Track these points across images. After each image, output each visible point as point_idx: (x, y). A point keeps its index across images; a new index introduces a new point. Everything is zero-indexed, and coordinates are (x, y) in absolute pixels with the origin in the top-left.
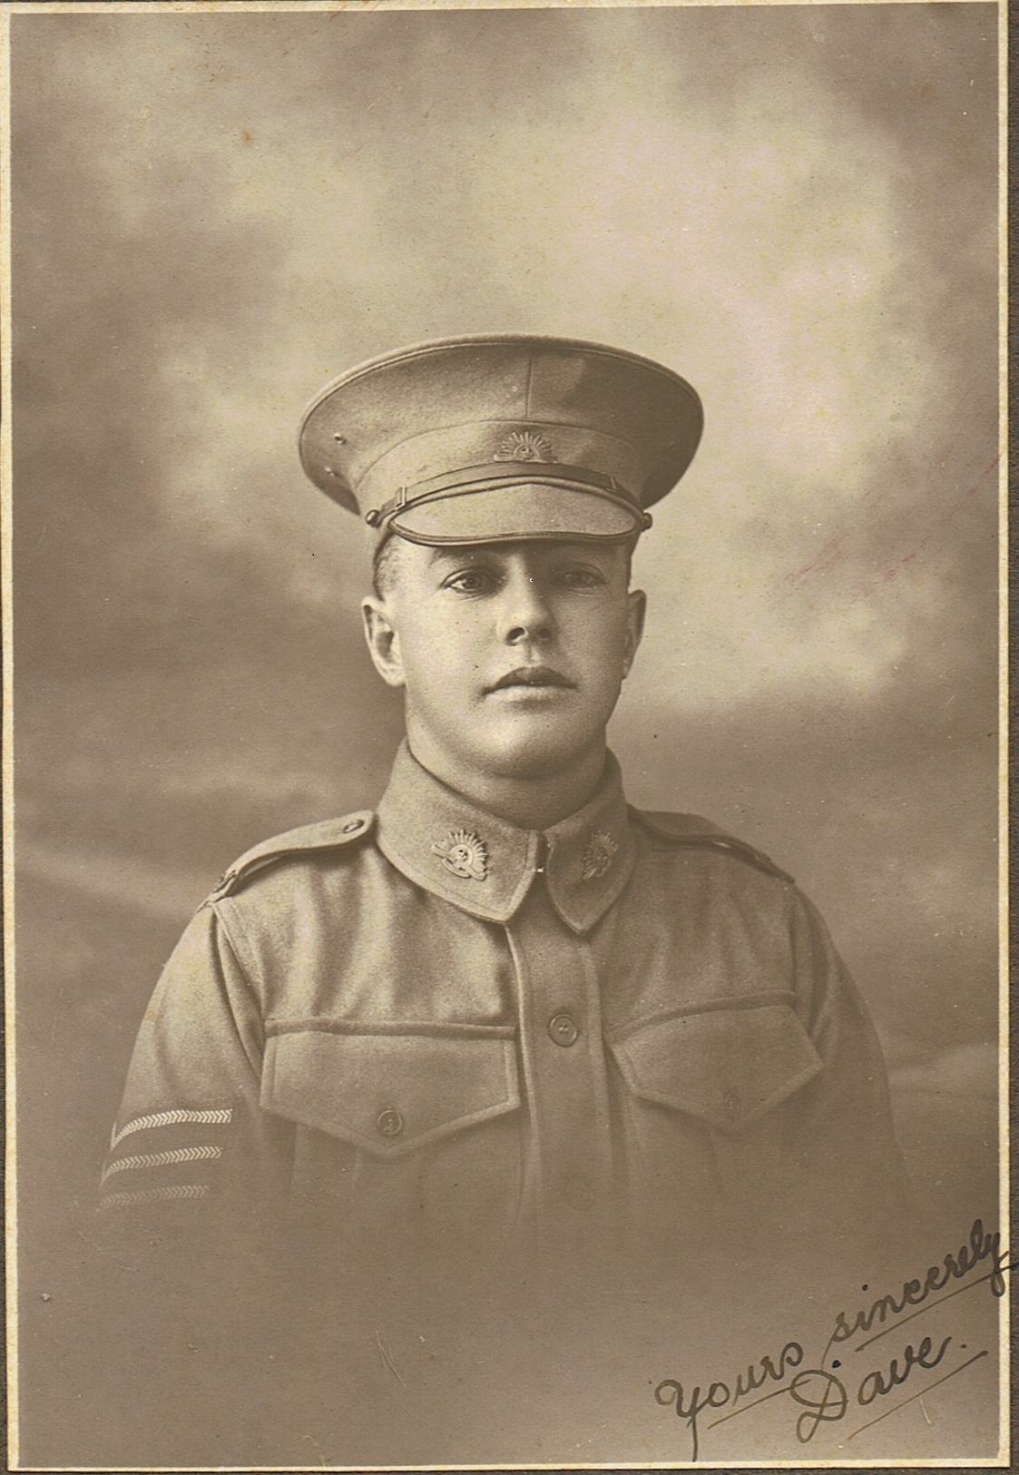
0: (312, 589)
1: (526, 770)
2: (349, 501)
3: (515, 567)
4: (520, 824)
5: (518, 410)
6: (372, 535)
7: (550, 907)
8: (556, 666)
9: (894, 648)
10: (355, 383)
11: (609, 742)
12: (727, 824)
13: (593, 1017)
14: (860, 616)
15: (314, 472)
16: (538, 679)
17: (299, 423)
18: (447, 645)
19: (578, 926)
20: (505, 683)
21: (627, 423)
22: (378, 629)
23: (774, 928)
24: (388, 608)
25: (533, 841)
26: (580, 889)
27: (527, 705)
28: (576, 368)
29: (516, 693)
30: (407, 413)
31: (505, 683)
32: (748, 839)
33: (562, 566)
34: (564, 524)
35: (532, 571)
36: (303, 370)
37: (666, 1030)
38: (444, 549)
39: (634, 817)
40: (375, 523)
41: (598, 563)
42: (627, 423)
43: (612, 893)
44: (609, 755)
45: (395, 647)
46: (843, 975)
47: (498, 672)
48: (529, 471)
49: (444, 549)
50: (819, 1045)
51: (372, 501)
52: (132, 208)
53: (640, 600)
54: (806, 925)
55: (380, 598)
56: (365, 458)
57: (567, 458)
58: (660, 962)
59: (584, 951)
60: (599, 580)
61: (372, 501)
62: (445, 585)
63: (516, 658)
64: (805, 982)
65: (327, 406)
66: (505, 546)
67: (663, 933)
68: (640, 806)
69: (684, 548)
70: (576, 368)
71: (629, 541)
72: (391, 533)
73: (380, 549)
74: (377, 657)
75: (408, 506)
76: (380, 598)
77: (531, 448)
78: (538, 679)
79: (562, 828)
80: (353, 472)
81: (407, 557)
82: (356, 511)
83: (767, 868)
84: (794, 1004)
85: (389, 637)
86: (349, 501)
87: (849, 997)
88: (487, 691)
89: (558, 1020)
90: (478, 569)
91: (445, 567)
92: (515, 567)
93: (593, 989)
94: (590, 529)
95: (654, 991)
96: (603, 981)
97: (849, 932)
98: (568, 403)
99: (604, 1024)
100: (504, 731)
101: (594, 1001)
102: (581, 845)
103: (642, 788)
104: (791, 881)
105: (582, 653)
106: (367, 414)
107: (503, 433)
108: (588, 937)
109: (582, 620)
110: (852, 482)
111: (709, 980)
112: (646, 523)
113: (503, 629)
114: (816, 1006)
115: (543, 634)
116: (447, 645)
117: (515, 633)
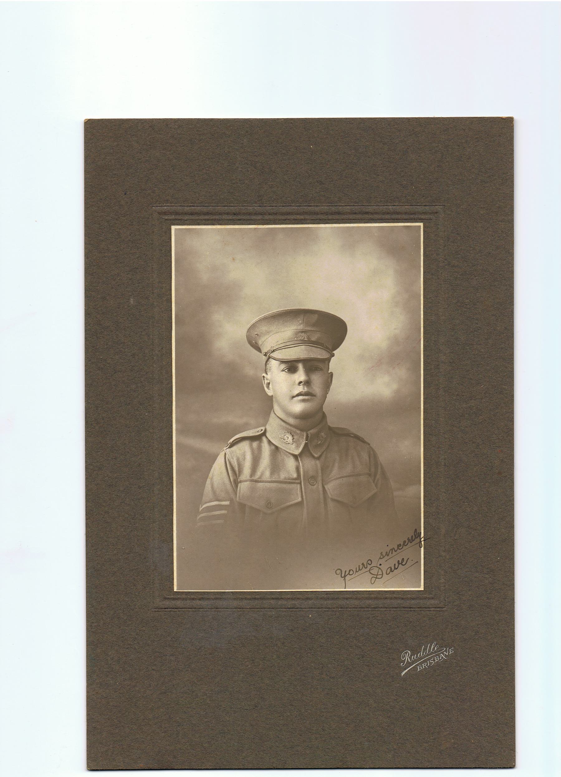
0: (250, 371)
1: (303, 417)
2: (259, 350)
3: (300, 366)
4: (302, 430)
5: (301, 327)
6: (265, 358)
7: (309, 451)
8: (310, 391)
9: (395, 386)
10: (260, 320)
11: (324, 410)
12: (353, 430)
13: (320, 478)
14: (386, 378)
15: (250, 343)
16: (306, 394)
17: (246, 330)
18: (283, 385)
19: (316, 456)
20: (298, 395)
21: (328, 330)
22: (266, 381)
23: (365, 456)
24: (269, 376)
25: (305, 434)
26: (317, 446)
27: (303, 401)
28: (316, 317)
29: (301, 398)
30: (273, 328)
31: (298, 395)
32: (359, 434)
33: (313, 366)
34: (313, 356)
35: (305, 367)
36: (247, 317)
37: (338, 482)
38: (283, 362)
39: (330, 428)
40: (265, 355)
41: (321, 365)
42: (328, 330)
43: (324, 448)
44: (324, 413)
45: (270, 386)
46: (382, 468)
47: (296, 392)
48: (303, 342)
49: (283, 362)
50: (376, 486)
51: (264, 350)
52: (205, 277)
53: (332, 374)
54: (373, 455)
55: (267, 374)
56: (263, 339)
57: (313, 339)
58: (337, 465)
59: (318, 462)
60: (321, 370)
61: (264, 350)
62: (283, 371)
63: (300, 389)
64: (373, 470)
65: (254, 326)
66: (298, 361)
67: (337, 457)
68: (331, 426)
69: (343, 361)
70: (316, 317)
71: (329, 360)
72: (269, 358)
73: (267, 362)
74: (266, 389)
75: (274, 351)
76: (267, 374)
77: (304, 336)
78: (306, 394)
79: (312, 431)
80: (260, 342)
81: (274, 364)
82: (261, 352)
83: (363, 441)
84: (370, 475)
85: (269, 384)
86: (259, 350)
87: (383, 473)
88: (293, 397)
89: (311, 479)
90: (291, 367)
91: (283, 366)
92: (300, 366)
93: (320, 471)
94: (319, 357)
95: (335, 472)
96: (322, 470)
97: (383, 457)
98: (314, 325)
99: (322, 480)
100: (298, 407)
101: (320, 474)
102: (317, 435)
103: (332, 421)
104: (369, 444)
105: (317, 388)
106: (263, 328)
107: (297, 333)
108: (318, 458)
109: (317, 379)
110: (384, 345)
111: (349, 469)
112: (333, 355)
113: (297, 382)
114: (375, 476)
115: (307, 383)
116: (283, 385)
117: (300, 383)
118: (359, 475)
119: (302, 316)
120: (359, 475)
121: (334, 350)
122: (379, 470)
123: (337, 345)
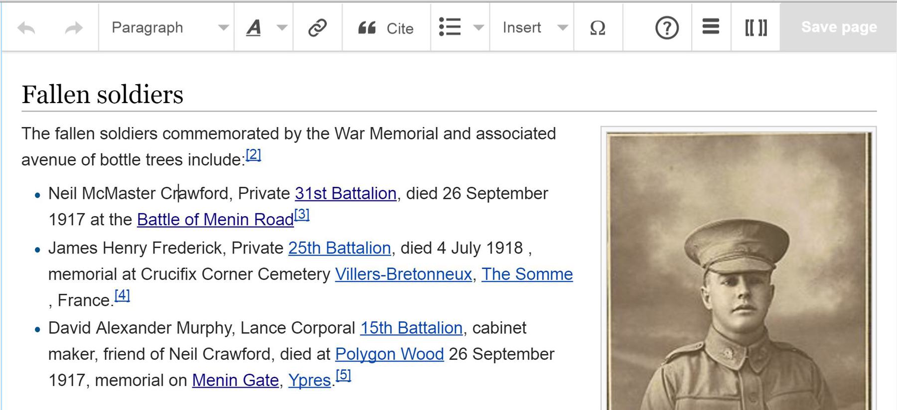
0: (688, 284)
1: (743, 331)
2: (698, 262)
3: (741, 279)
4: (742, 345)
5: (741, 238)
6: (704, 271)
7: (750, 367)
8: (751, 304)
9: (839, 300)
10: (699, 231)
11: (765, 324)
12: (796, 346)
13: (761, 395)
14: (830, 292)
15: (689, 255)
16: (747, 308)
17: (684, 241)
18: (723, 299)
19: (757, 371)
20: (738, 309)
21: (769, 242)
22: (705, 295)
23: (808, 372)
24: (708, 289)
25: (745, 349)
26: (758, 361)
27: (744, 314)
28: (756, 227)
29: (741, 311)
30: (712, 239)
31: (738, 309)
32: (803, 350)
33: (753, 278)
34: (754, 268)
35: (745, 279)
36: (686, 228)
37: (780, 398)
38: (722, 274)
39: (772, 343)
40: (704, 267)
41: (762, 278)
42: (769, 242)
43: (765, 363)
44: (765, 327)
45: (710, 299)
46: (825, 384)
47: (736, 306)
48: (744, 254)
49: (722, 274)
50: (819, 403)
51: (703, 262)
52: (641, 187)
53: (773, 287)
54: (816, 371)
55: (705, 286)
56: (701, 251)
57: (754, 251)
58: (778, 381)
59: (758, 378)
60: (762, 282)
61: (703, 262)
62: (723, 283)
63: (741, 302)
64: (816, 386)
65: (692, 237)
66: (738, 273)
67: (779, 373)
68: (774, 340)
69: (785, 273)
70: (756, 227)
71: (770, 272)
72: (709, 270)
73: (705, 276)
74: (705, 302)
75: (713, 263)
76: (705, 286)
77: (745, 248)
78: (747, 308)
79: (753, 346)
80: (699, 255)
81: (713, 276)
82: (699, 263)
83: (807, 357)
84: (812, 391)
85: (708, 297)
86: (698, 262)
87: (827, 390)
88: (734, 311)
89: (752, 396)
90: (731, 279)
91: (723, 279)
92: (741, 279)
93: (761, 388)
94: (761, 269)
95: (777, 388)
96: (763, 385)
97: (826, 374)
98: (754, 236)
99: (764, 397)
100: (738, 321)
101: (761, 390)
102: (758, 349)
103: (773, 336)
104: (811, 359)
105: (758, 302)
106: (702, 239)
107: (736, 245)
108: (759, 374)
109: (758, 292)
110: (827, 257)
111: (791, 385)
112: (775, 267)
113: (738, 295)
114: (818, 392)
115: (748, 296)
116: (723, 299)
117: (740, 296)
118: (802, 391)
119: (742, 228)
120: (802, 391)
121: (776, 261)
122: (823, 388)
123: (778, 257)
